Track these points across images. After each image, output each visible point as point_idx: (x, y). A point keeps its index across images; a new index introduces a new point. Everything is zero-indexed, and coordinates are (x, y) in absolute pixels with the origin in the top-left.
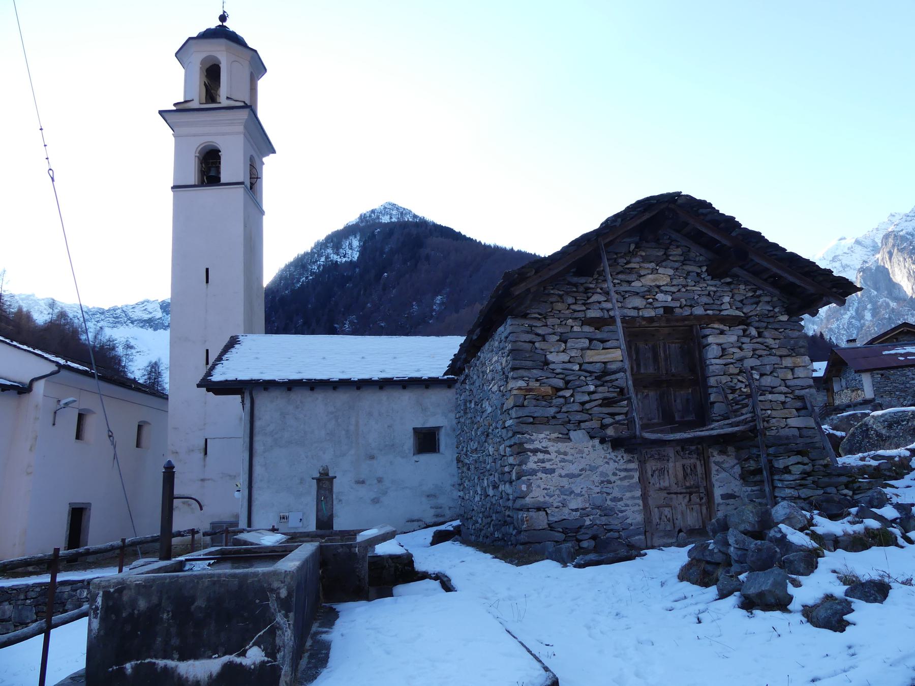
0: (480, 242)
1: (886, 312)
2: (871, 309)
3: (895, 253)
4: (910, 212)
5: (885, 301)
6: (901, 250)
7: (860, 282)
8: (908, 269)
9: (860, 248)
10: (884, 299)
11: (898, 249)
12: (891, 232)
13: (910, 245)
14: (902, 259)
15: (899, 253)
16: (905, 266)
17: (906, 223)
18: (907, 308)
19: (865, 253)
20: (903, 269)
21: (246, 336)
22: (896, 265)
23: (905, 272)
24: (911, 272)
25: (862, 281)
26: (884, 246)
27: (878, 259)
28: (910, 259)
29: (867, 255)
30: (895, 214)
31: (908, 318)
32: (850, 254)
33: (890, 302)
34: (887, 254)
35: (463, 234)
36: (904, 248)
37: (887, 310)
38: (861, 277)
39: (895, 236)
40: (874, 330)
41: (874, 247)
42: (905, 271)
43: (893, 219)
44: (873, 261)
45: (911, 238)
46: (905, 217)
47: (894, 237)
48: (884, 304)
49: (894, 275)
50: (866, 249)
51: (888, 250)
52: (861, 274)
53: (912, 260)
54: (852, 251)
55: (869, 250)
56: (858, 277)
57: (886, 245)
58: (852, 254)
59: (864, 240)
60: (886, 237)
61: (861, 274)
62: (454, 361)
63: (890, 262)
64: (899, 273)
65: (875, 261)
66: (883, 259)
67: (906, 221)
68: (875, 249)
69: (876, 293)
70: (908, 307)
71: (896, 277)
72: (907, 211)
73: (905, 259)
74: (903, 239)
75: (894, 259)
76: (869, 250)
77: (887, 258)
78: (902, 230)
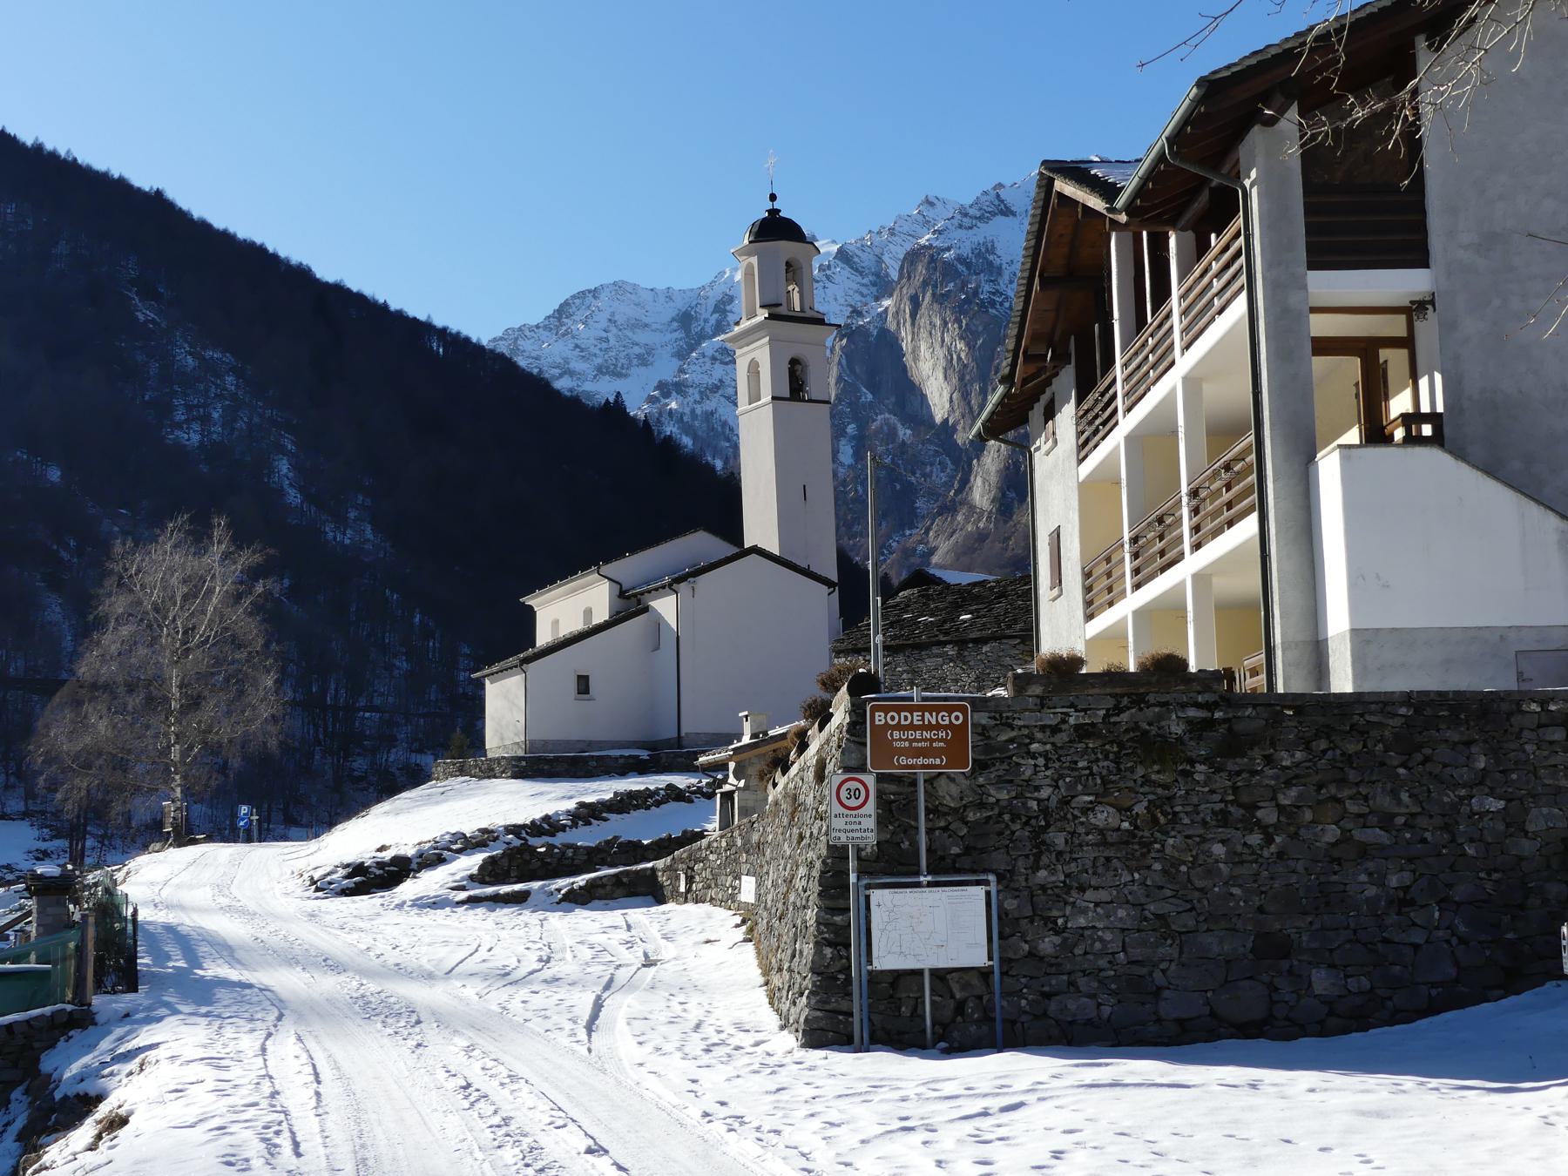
0: (385, 306)
1: (887, 450)
2: (854, 437)
3: (926, 302)
4: (971, 206)
5: (886, 421)
6: (939, 299)
7: (840, 363)
8: (949, 349)
9: (847, 272)
10: (887, 415)
11: (934, 295)
12: (924, 247)
13: (962, 290)
14: (938, 322)
15: (936, 306)
16: (943, 341)
17: (960, 230)
18: (932, 448)
19: (856, 287)
20: (937, 346)
21: (115, 1137)
22: (924, 334)
23: (941, 356)
24: (955, 357)
25: (844, 362)
26: (905, 280)
27: (887, 308)
28: (956, 326)
29: (862, 295)
30: (936, 201)
31: (932, 472)
32: (821, 283)
33: (899, 426)
34: (908, 303)
35: (271, 250)
36: (946, 296)
37: (890, 446)
38: (842, 348)
39: (932, 259)
40: (856, 491)
41: (877, 275)
42: (941, 353)
43: (930, 213)
44: (874, 313)
45: (966, 272)
46: (959, 217)
47: (929, 263)
48: (885, 428)
49: (916, 359)
50: (859, 279)
51: (912, 291)
52: (845, 341)
53: (960, 327)
54: (828, 277)
55: (866, 281)
56: (837, 348)
57: (909, 278)
58: (828, 284)
59: (859, 253)
60: (912, 257)
61: (845, 341)
62: (760, 965)
63: (913, 324)
64: (928, 356)
65: (880, 315)
66: (897, 312)
67: (960, 226)
68: (883, 287)
69: (870, 397)
70: (936, 445)
71: (921, 364)
72: (967, 200)
73: (945, 323)
74: (949, 270)
75: (923, 321)
76: (866, 281)
77: (907, 311)
78: (948, 249)
